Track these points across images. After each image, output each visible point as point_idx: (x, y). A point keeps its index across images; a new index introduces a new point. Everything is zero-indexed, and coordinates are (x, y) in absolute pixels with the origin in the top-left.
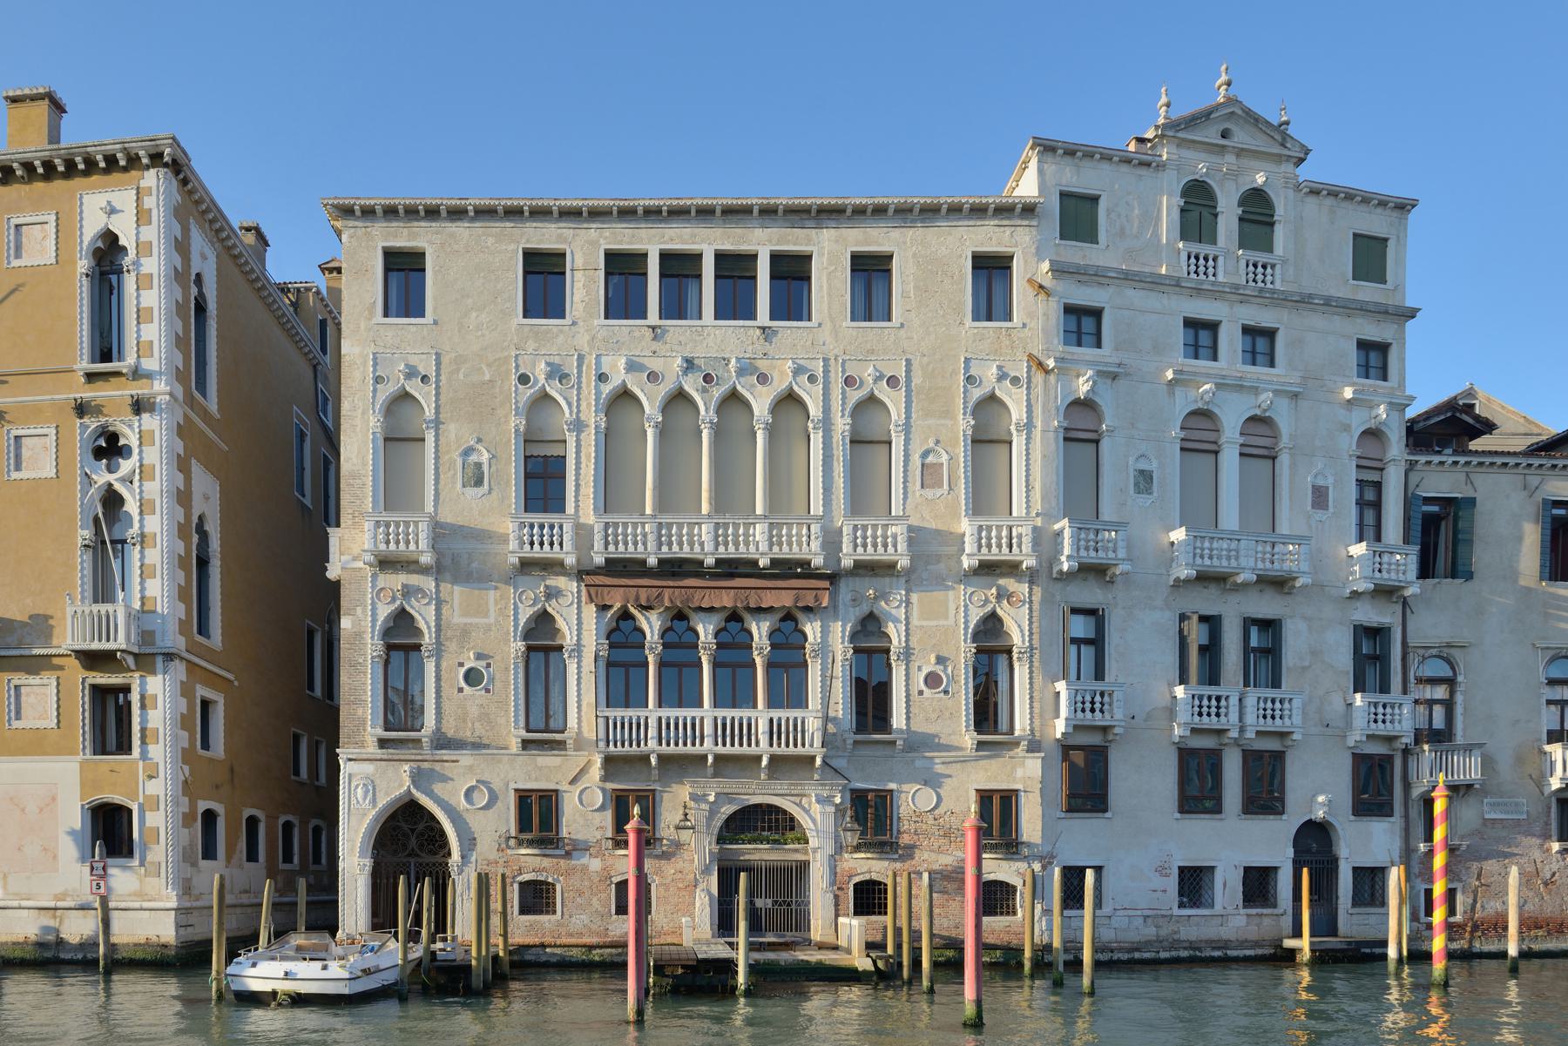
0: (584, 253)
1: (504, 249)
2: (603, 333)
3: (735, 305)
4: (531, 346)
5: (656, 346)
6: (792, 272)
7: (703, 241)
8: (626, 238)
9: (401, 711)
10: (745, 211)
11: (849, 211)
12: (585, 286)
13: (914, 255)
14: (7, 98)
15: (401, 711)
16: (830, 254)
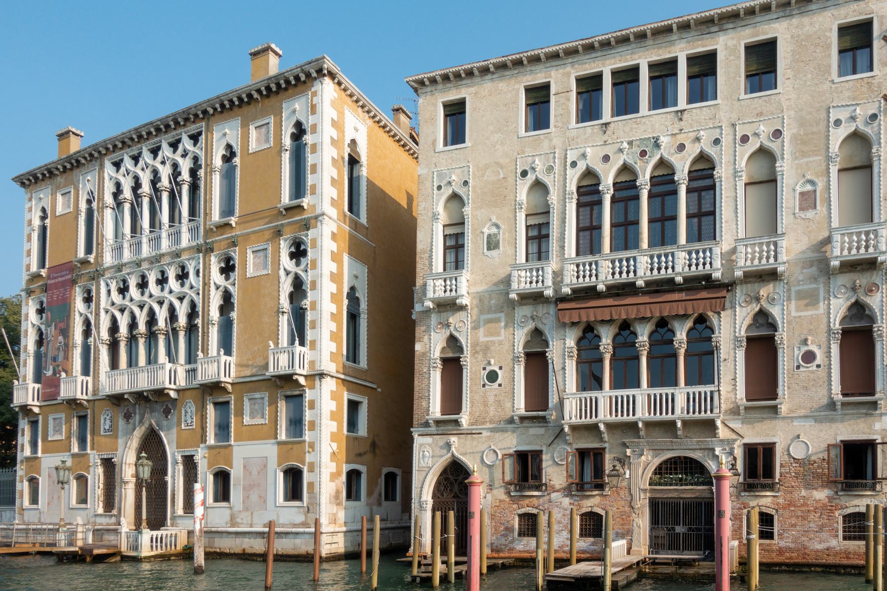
0: (563, 81)
1: (512, 92)
2: (573, 133)
3: (662, 99)
4: (529, 151)
5: (605, 137)
6: (704, 67)
7: (640, 58)
8: (588, 67)
9: (453, 398)
10: (668, 30)
11: (742, 13)
12: (564, 103)
13: (792, 37)
14: (251, 54)
15: (453, 398)
16: (730, 49)
